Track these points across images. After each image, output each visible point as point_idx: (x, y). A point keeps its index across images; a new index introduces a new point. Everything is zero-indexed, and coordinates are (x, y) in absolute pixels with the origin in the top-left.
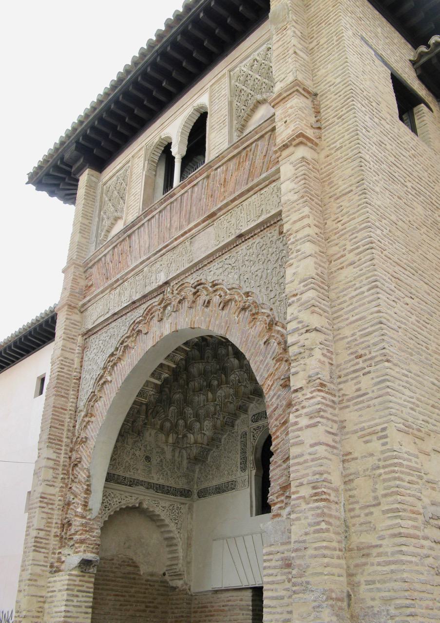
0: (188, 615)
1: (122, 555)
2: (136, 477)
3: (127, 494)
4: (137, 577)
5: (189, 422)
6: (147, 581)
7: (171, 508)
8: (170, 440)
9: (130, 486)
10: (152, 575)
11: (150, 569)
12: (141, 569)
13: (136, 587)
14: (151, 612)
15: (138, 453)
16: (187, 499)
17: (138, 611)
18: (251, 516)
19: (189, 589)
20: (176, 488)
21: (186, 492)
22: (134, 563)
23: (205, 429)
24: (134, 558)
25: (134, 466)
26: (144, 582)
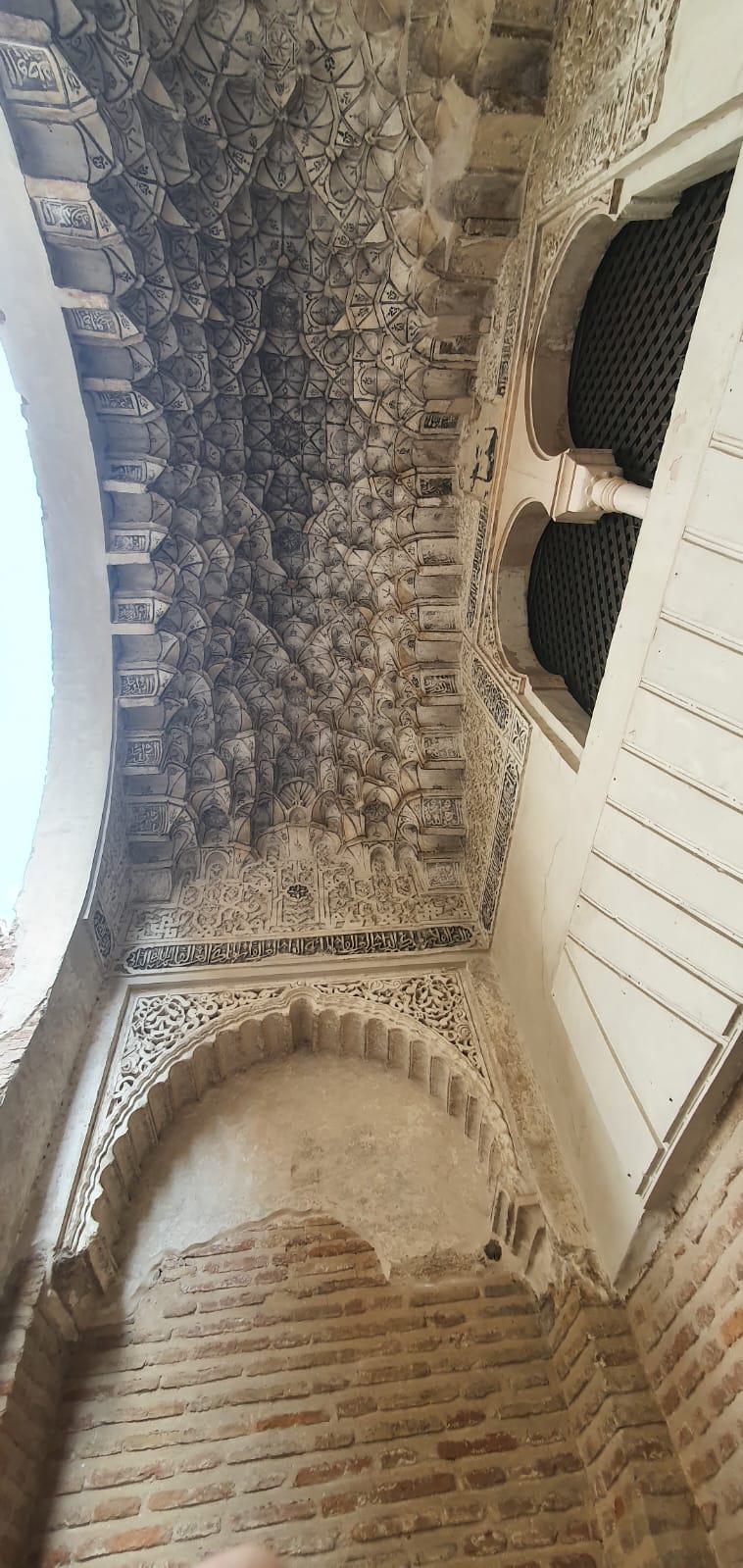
0: (648, 1435)
1: (287, 1217)
2: (262, 935)
3: (239, 988)
4: (369, 1295)
5: (364, 766)
6: (422, 1301)
7: (412, 989)
8: (350, 833)
9: (241, 959)
10: (435, 1266)
11: (421, 1247)
12: (379, 1254)
13: (372, 1352)
14: (481, 1479)
15: (263, 887)
16: (457, 948)
17: (405, 1490)
18: (574, 764)
19: (592, 1272)
20: (406, 933)
21: (447, 934)
22: (342, 1234)
23: (407, 754)
24: (342, 1218)
25: (253, 916)
26: (404, 1312)
